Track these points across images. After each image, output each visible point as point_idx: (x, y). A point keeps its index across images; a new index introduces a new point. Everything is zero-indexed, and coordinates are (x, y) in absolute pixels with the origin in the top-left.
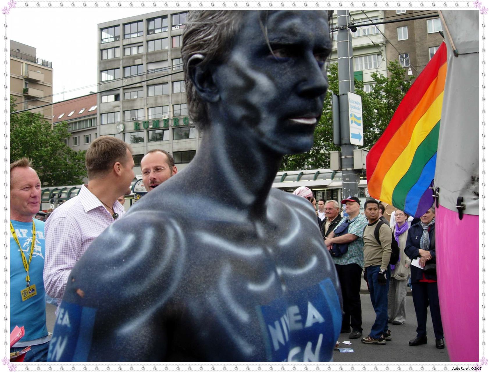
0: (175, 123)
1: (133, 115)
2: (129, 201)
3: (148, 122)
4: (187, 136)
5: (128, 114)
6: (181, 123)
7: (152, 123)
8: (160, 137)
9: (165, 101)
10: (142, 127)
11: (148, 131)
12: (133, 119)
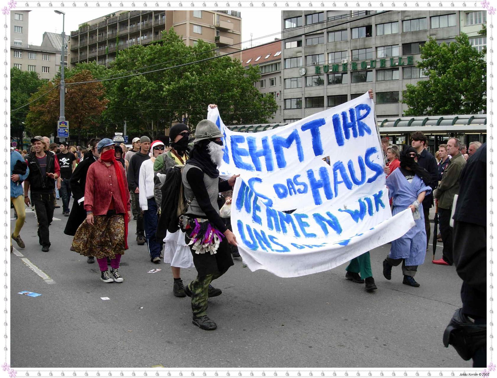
0: (353, 67)
1: (314, 60)
3: (328, 66)
5: (309, 58)
6: (359, 67)
7: (332, 68)
9: (344, 46)
10: (322, 71)
11: (328, 75)
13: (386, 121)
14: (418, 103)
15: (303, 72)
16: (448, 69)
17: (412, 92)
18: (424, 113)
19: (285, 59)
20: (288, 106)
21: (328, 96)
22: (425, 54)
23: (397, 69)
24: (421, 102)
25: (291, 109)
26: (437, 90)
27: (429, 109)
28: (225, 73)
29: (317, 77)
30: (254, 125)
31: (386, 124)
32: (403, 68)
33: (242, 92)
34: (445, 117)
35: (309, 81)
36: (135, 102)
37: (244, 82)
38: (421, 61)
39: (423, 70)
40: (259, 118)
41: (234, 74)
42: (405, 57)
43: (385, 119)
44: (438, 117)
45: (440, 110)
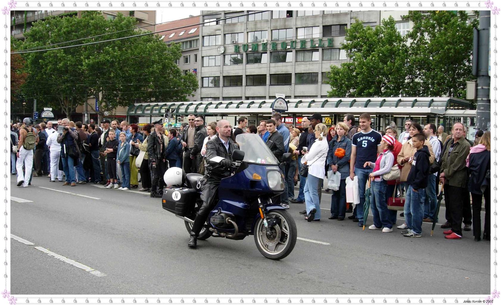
0: (273, 47)
2: (234, 118)
4: (284, 59)
5: (228, 37)
6: (279, 48)
7: (251, 47)
8: (258, 60)
10: (241, 50)
11: (247, 54)
12: (233, 42)
13: (314, 101)
14: (341, 85)
15: (222, 50)
16: (372, 52)
17: (336, 72)
18: (347, 94)
19: (203, 37)
20: (206, 84)
21: (247, 76)
22: (350, 36)
23: (318, 50)
24: (344, 83)
25: (208, 87)
26: (361, 72)
27: (352, 91)
28: (146, 48)
29: (236, 56)
30: (176, 103)
31: (313, 105)
32: (323, 49)
33: (163, 68)
34: (372, 99)
35: (228, 58)
36: (50, 76)
37: (166, 59)
38: (345, 42)
39: (347, 52)
40: (178, 96)
41: (155, 49)
42: (325, 39)
43: (312, 99)
44: (366, 99)
45: (364, 93)
